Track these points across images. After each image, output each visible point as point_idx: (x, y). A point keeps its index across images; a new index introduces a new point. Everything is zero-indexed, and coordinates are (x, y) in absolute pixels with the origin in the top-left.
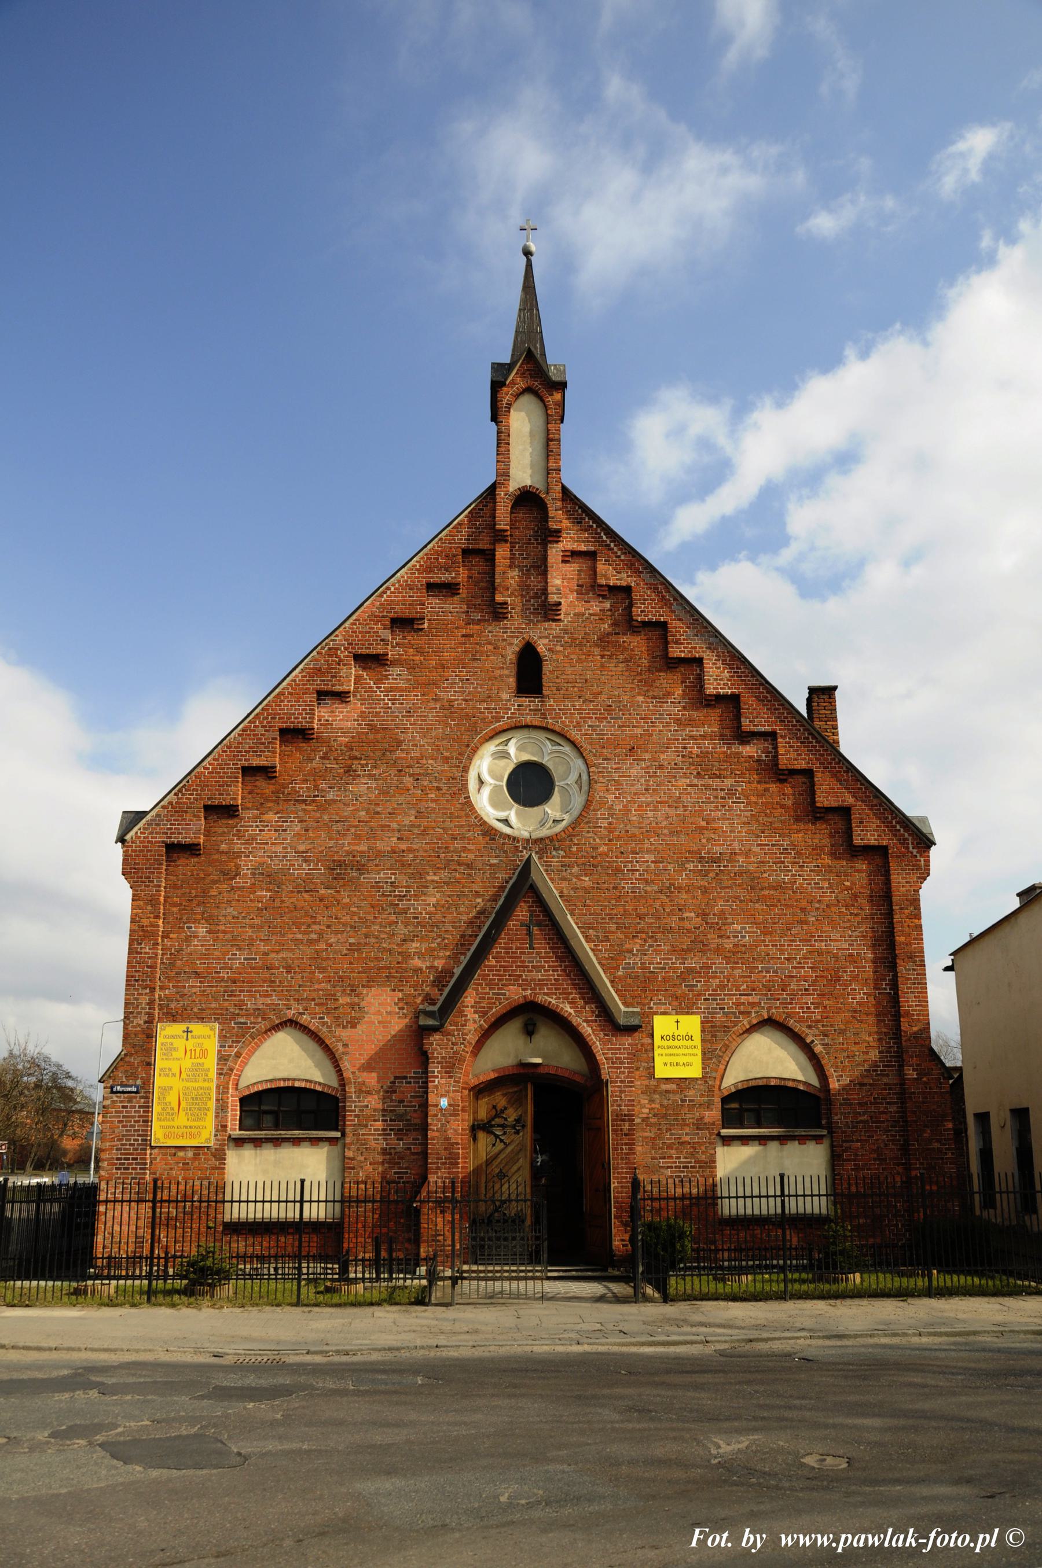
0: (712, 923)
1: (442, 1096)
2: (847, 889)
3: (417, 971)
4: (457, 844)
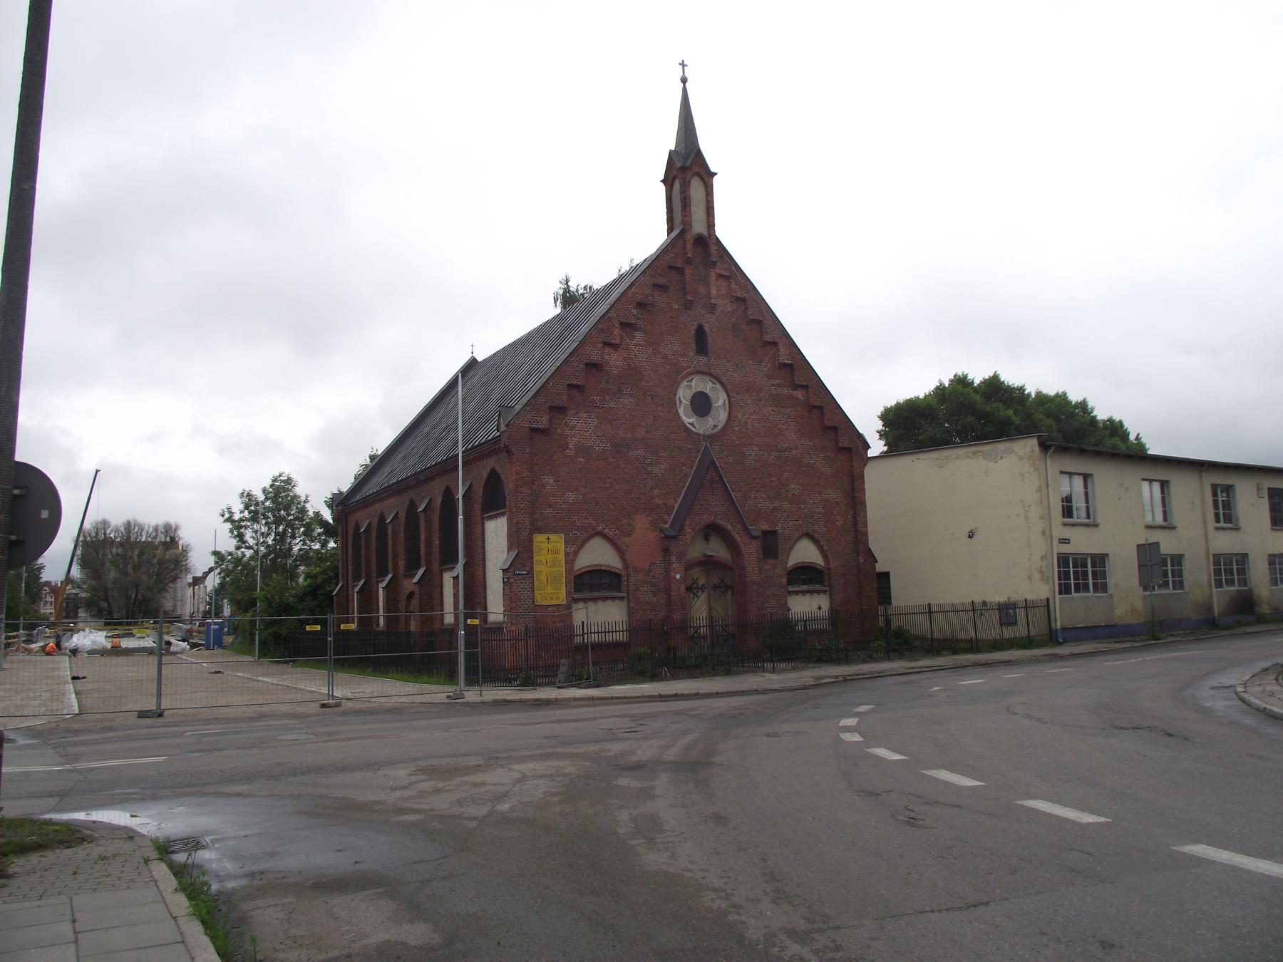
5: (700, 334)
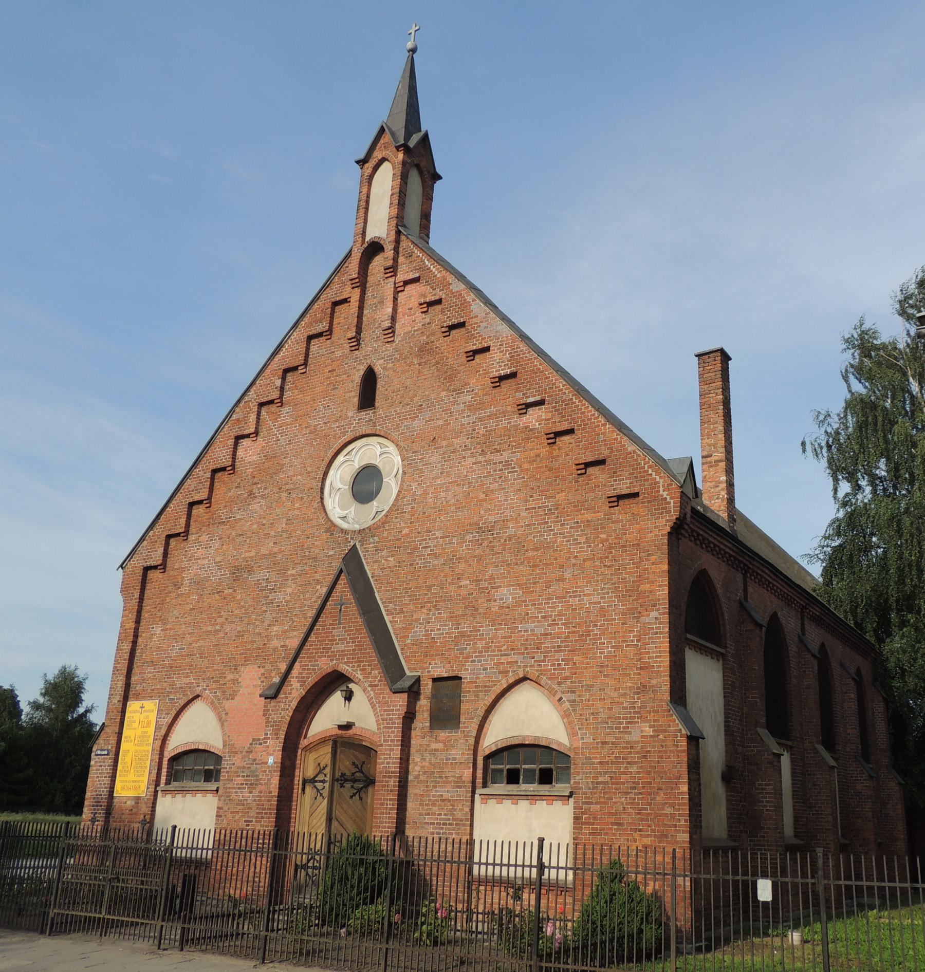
0: (483, 588)
1: (271, 755)
2: (603, 541)
3: (275, 650)
4: (309, 542)
5: (370, 381)
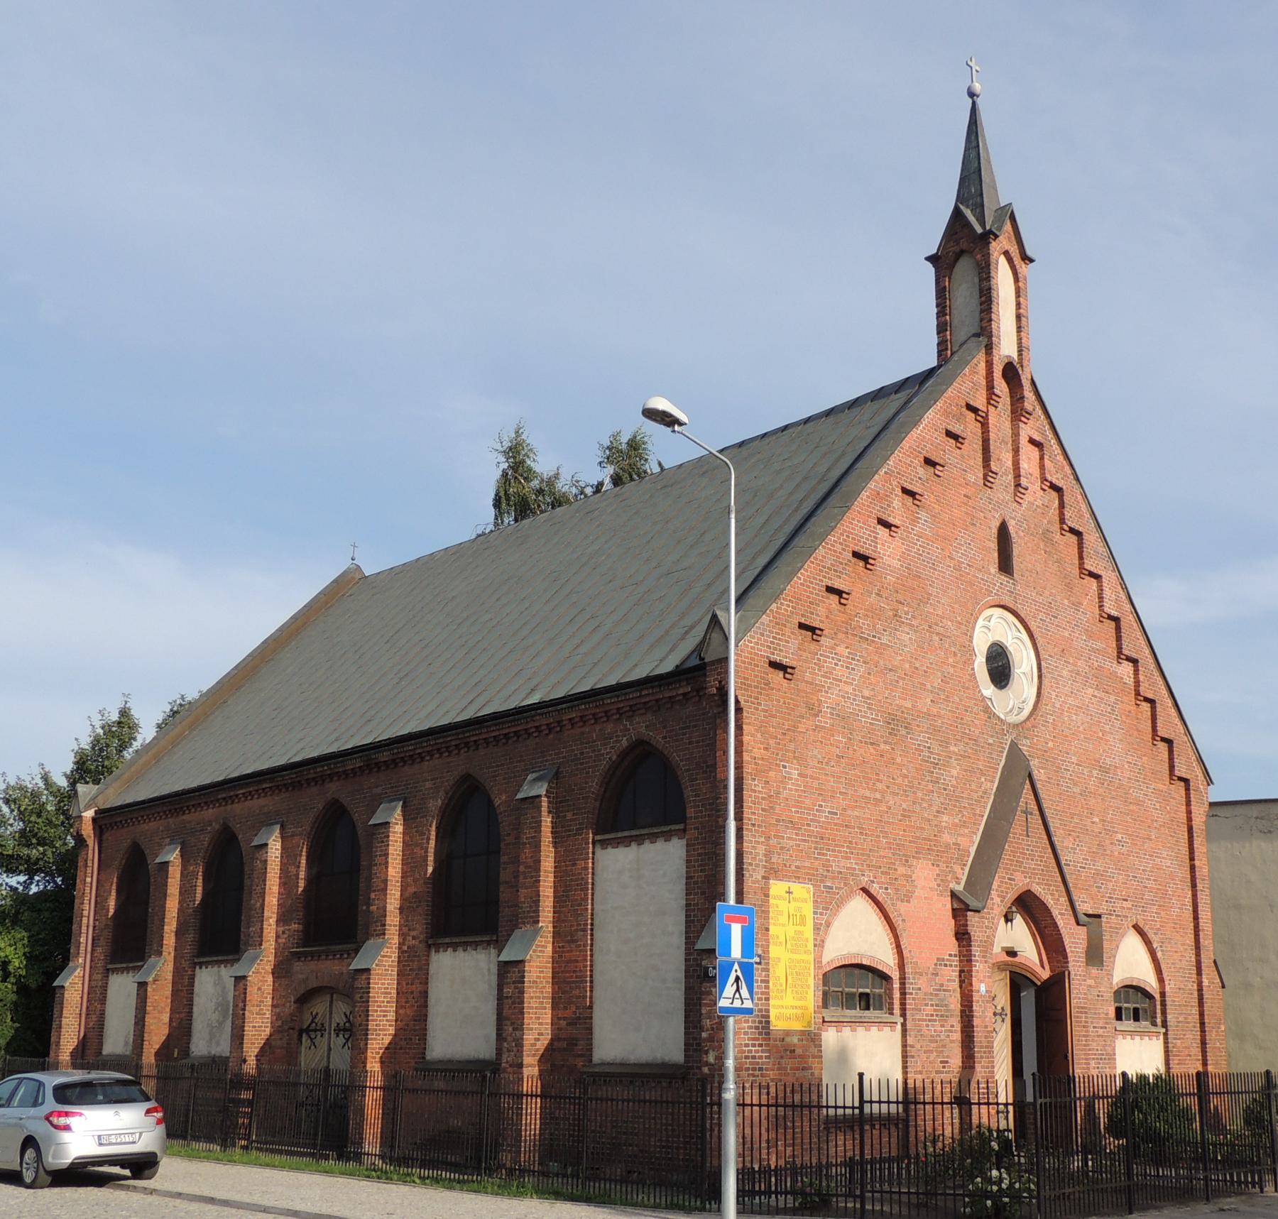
3: (948, 846)
